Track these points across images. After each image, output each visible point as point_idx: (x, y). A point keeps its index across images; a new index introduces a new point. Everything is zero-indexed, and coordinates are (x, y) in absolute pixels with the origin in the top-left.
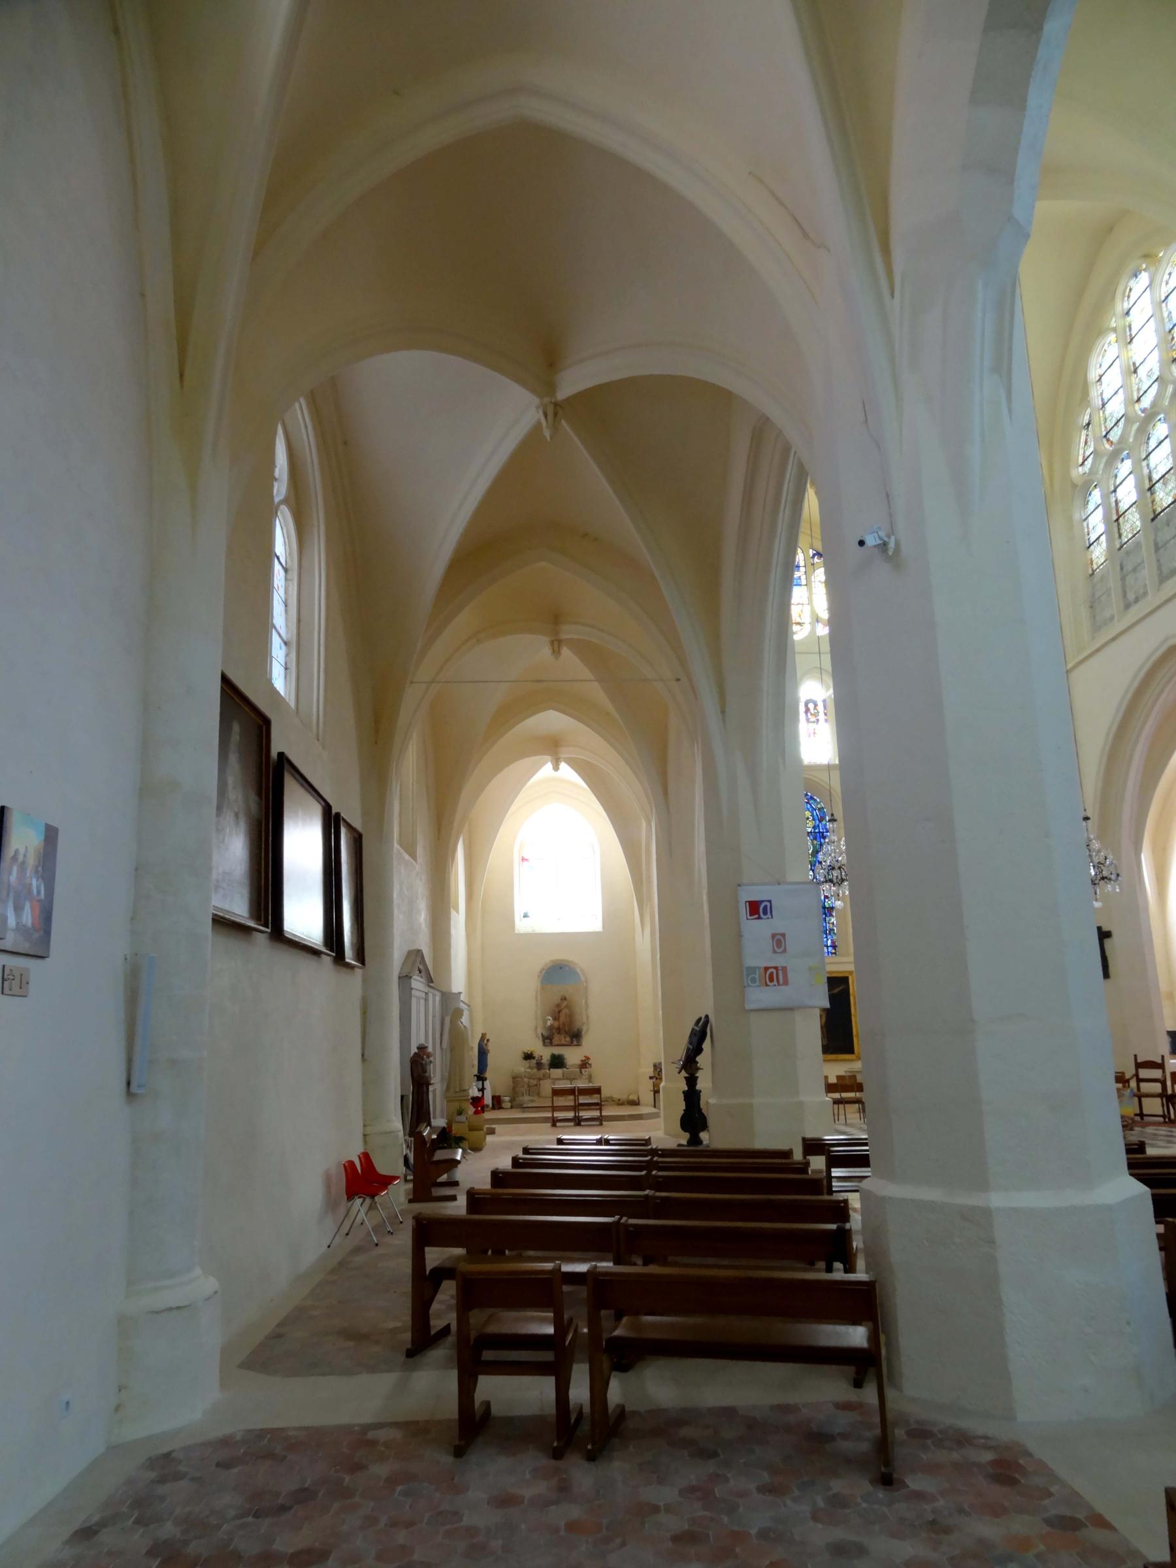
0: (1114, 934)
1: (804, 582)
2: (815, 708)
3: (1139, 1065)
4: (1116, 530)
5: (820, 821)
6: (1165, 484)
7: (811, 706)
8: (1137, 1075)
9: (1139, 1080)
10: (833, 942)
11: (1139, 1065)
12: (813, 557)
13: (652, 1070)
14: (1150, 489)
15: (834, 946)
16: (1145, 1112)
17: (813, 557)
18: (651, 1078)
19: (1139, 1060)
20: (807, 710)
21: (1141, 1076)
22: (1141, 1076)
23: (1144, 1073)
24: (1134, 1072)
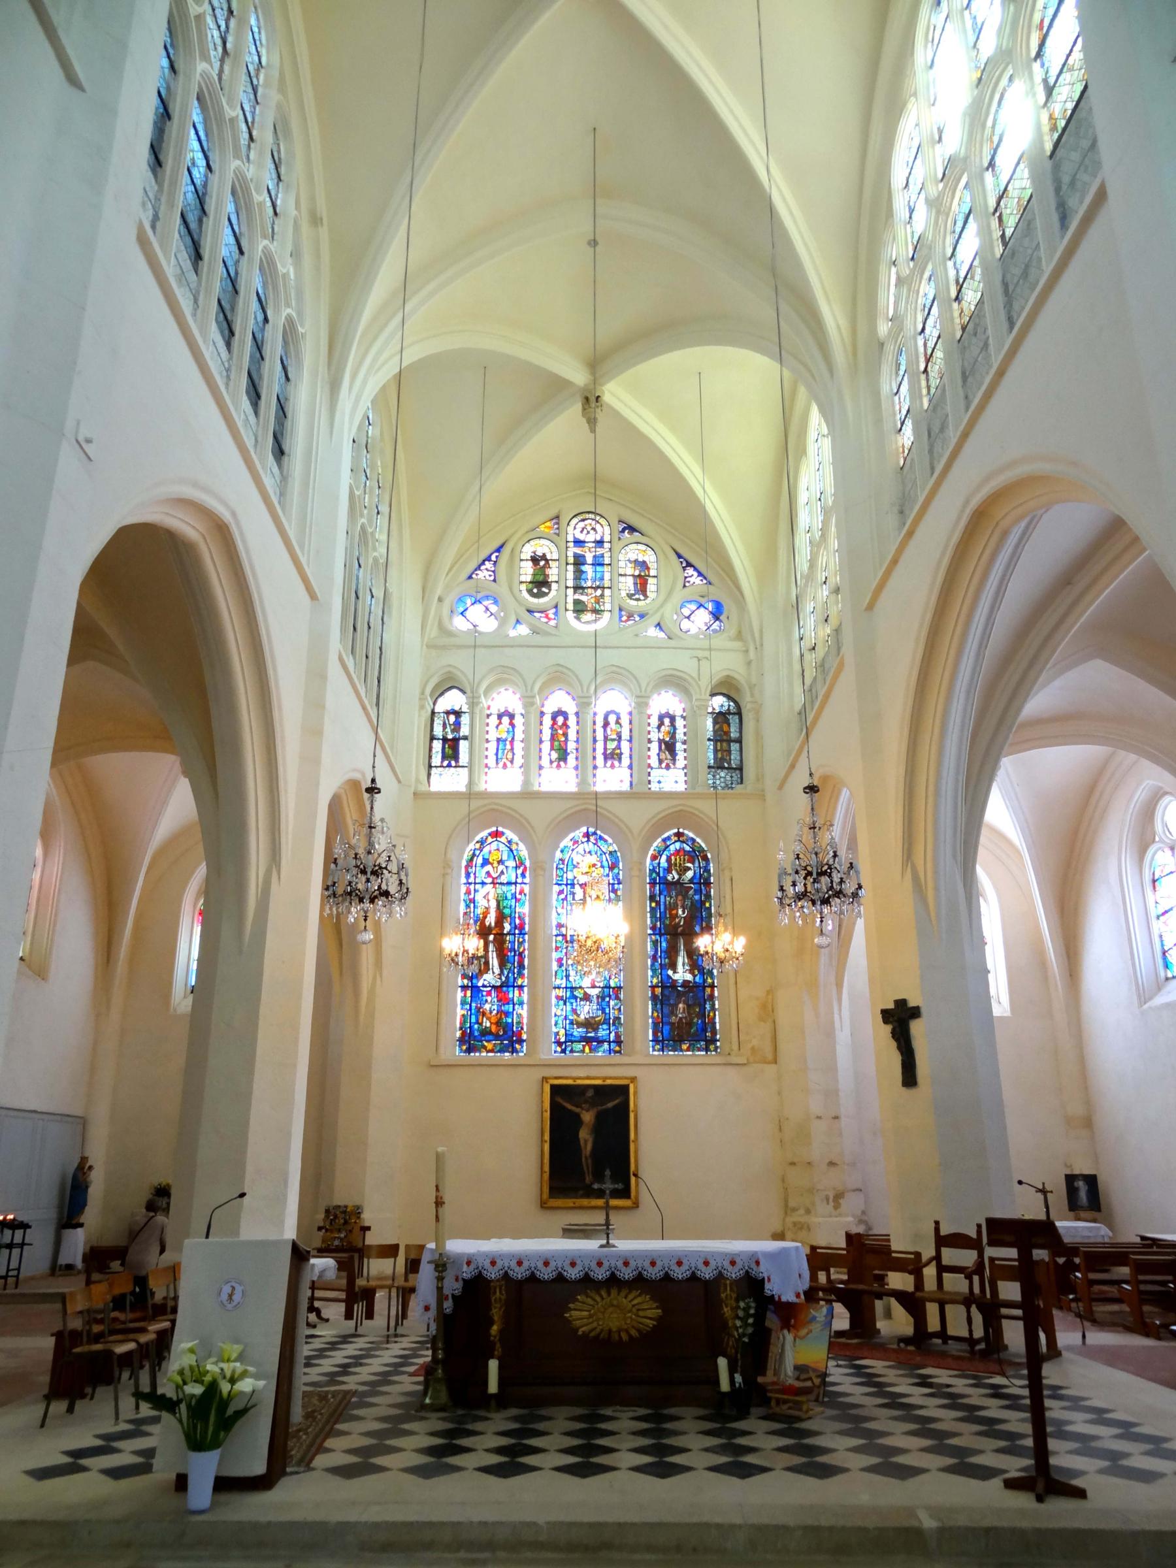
0: (923, 1010)
1: (607, 561)
2: (618, 722)
3: (942, 1241)
4: (924, 383)
5: (611, 868)
6: (972, 278)
7: (612, 719)
8: (938, 1258)
9: (942, 1269)
10: (617, 1036)
11: (942, 1241)
12: (623, 531)
13: (322, 1216)
14: (957, 298)
15: (618, 1042)
16: (951, 1332)
17: (623, 531)
18: (320, 1229)
19: (944, 1231)
20: (606, 724)
21: (946, 1261)
22: (946, 1261)
23: (950, 1256)
24: (933, 1253)
